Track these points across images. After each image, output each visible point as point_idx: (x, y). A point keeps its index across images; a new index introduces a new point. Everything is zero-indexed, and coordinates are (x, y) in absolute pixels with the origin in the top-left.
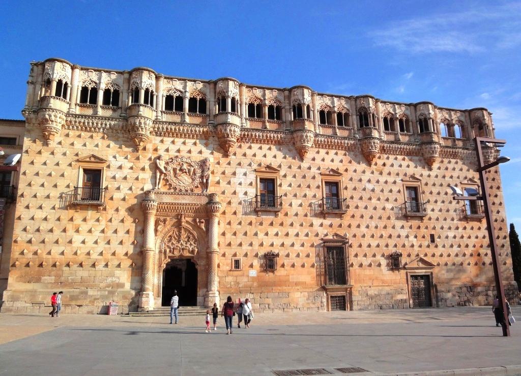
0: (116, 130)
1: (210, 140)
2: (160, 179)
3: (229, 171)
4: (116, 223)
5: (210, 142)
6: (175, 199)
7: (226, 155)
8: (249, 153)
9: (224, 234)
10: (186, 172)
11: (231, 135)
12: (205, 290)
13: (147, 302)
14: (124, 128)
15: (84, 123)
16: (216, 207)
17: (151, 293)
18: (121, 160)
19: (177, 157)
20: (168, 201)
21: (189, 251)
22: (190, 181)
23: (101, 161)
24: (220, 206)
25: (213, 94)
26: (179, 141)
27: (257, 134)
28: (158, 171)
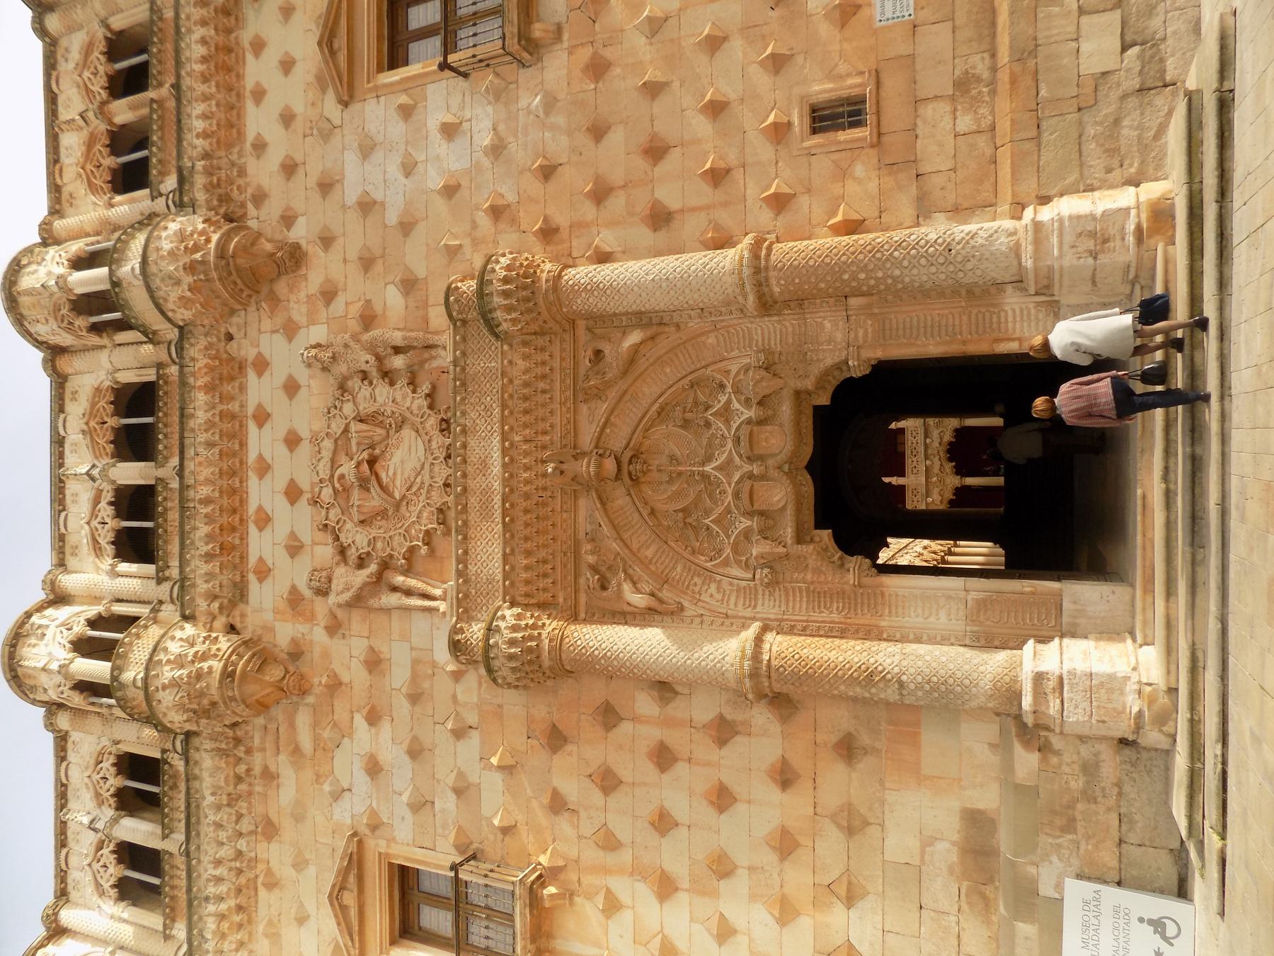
0: (239, 779)
1: (243, 353)
2: (408, 593)
3: (354, 237)
4: (624, 817)
5: (250, 353)
6: (486, 513)
7: (293, 258)
8: (280, 145)
9: (660, 218)
10: (372, 462)
11: (196, 248)
12: (1012, 301)
13: (1101, 687)
14: (224, 746)
15: (222, 917)
16: (506, 280)
17: (1040, 658)
18: (347, 764)
19: (315, 502)
20: (497, 550)
21: (761, 422)
22: (407, 433)
23: (354, 863)
24: (504, 261)
25: (89, 356)
26: (260, 493)
27: (199, 125)
28: (374, 603)
